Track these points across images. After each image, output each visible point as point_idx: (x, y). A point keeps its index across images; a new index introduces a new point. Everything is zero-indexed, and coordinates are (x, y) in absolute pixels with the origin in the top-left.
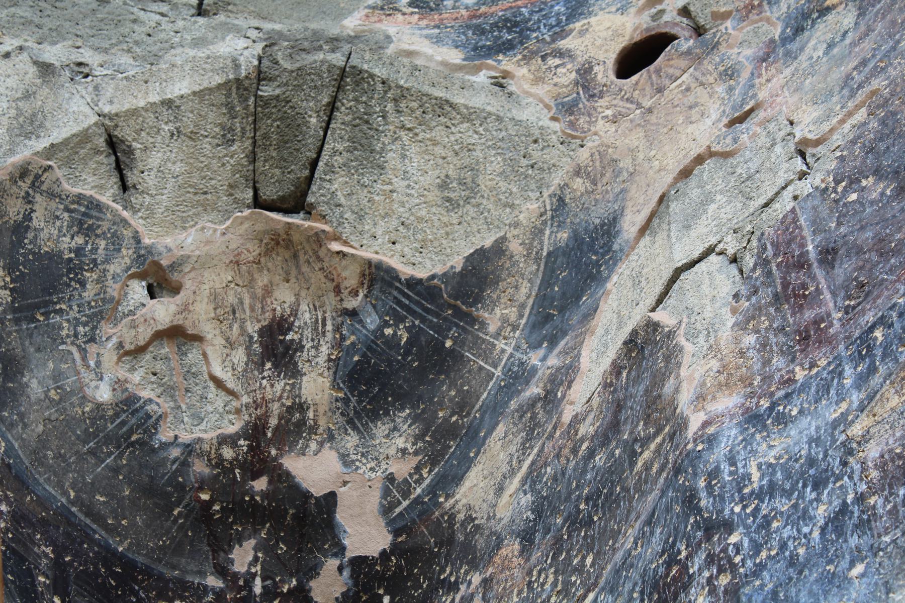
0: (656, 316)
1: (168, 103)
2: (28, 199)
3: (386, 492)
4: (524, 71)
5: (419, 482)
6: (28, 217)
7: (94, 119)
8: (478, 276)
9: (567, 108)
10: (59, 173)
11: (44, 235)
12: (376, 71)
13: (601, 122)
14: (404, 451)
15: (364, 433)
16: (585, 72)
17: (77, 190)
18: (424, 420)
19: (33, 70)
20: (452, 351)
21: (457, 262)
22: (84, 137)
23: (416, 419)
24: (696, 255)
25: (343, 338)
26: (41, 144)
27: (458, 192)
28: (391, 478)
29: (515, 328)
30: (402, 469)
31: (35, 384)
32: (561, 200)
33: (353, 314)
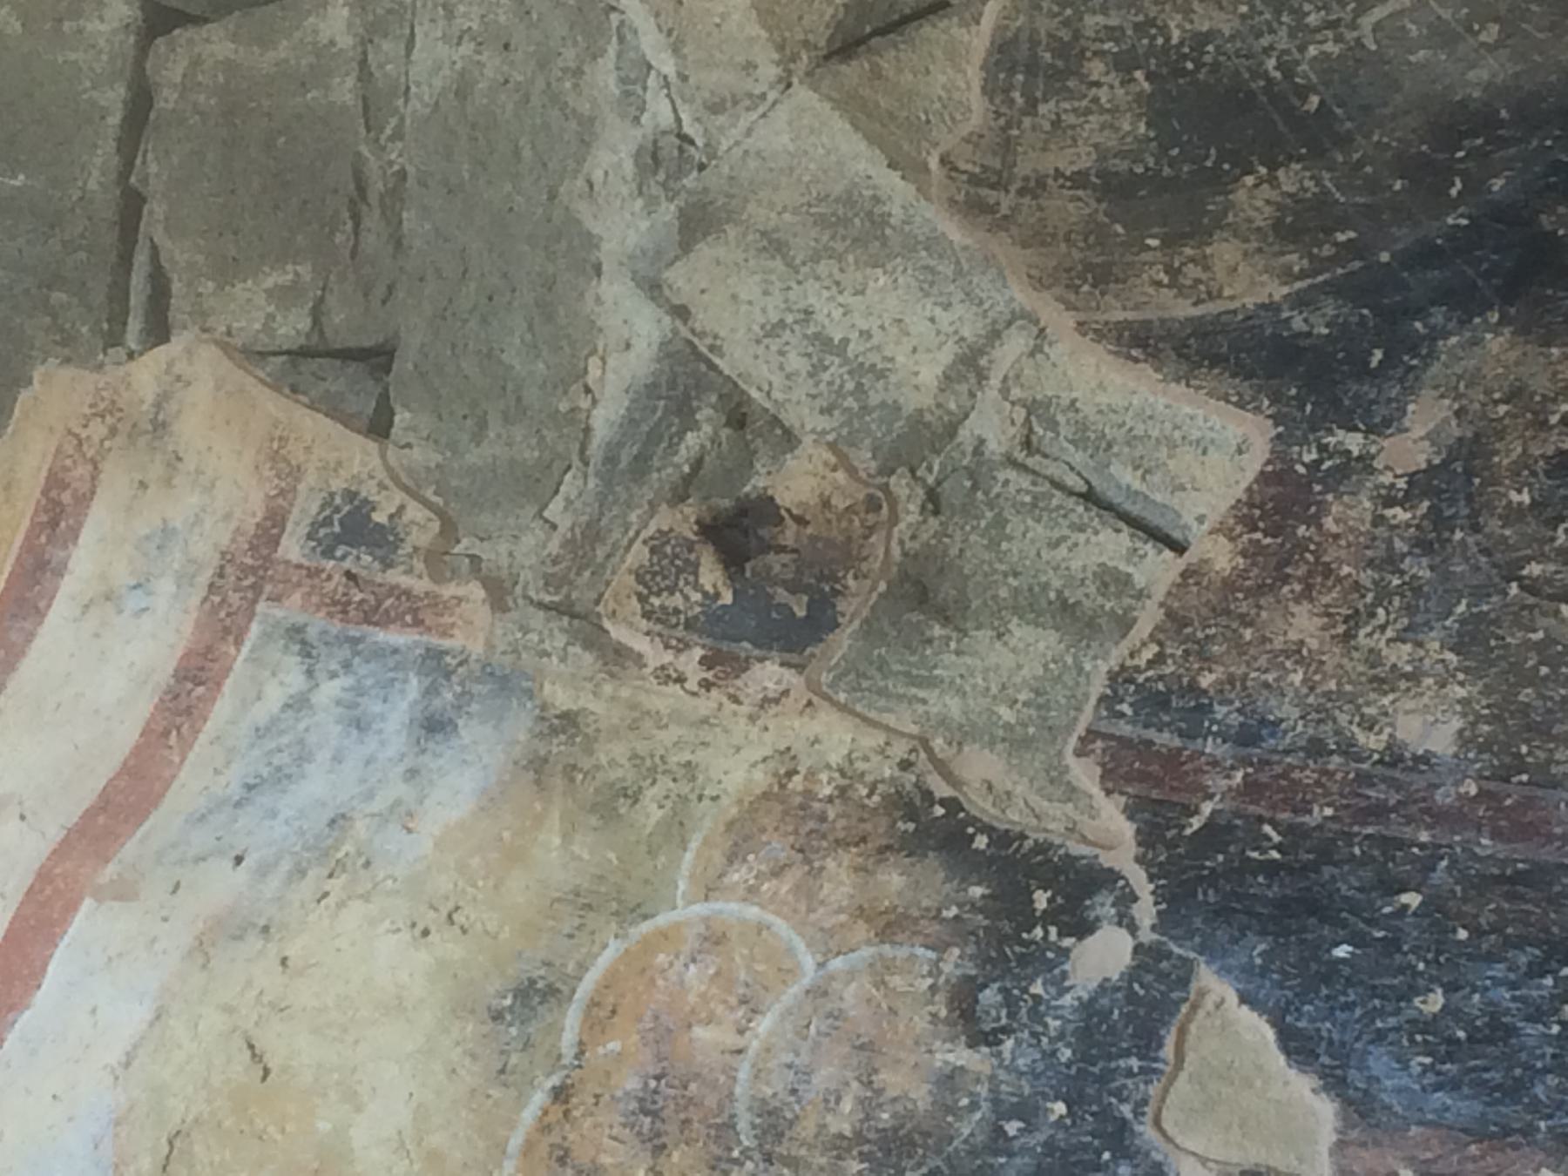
2: (1035, 187)
6: (1079, 180)
7: (802, 94)
10: (948, 141)
11: (1110, 141)
17: (977, 101)
19: (705, 251)
22: (856, 109)
26: (895, 189)
31: (1482, 73)
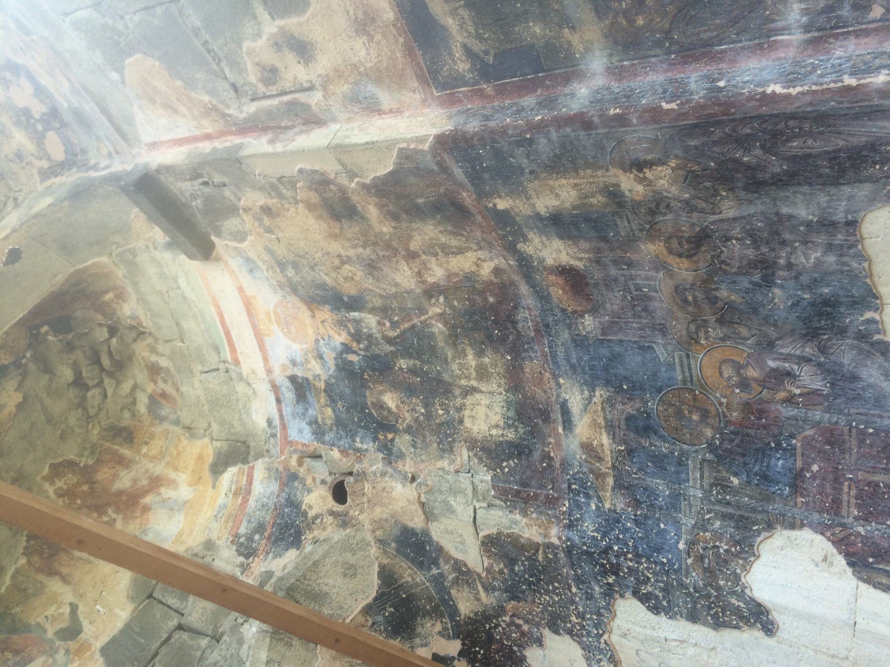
0: (481, 534)
1: (268, 662)
3: (443, 636)
4: (316, 532)
5: (446, 623)
8: (387, 577)
9: (344, 525)
12: (291, 582)
13: (359, 517)
14: (433, 625)
15: (418, 635)
16: (332, 513)
18: (426, 614)
20: (408, 596)
21: (376, 581)
23: (424, 616)
24: (472, 514)
25: (380, 630)
27: (350, 571)
28: (439, 632)
29: (416, 573)
30: (438, 627)
32: (379, 540)
33: (373, 624)
